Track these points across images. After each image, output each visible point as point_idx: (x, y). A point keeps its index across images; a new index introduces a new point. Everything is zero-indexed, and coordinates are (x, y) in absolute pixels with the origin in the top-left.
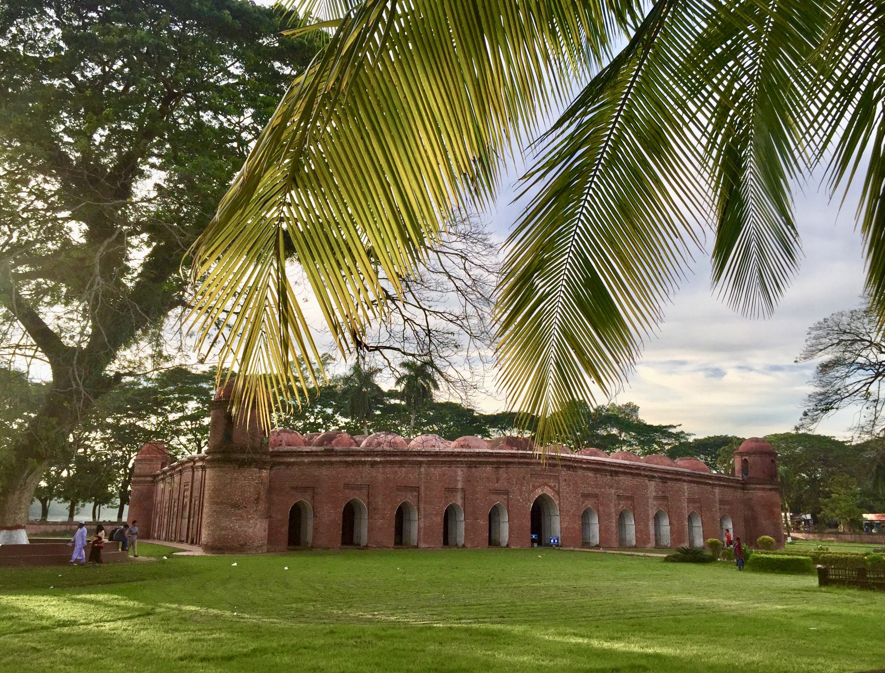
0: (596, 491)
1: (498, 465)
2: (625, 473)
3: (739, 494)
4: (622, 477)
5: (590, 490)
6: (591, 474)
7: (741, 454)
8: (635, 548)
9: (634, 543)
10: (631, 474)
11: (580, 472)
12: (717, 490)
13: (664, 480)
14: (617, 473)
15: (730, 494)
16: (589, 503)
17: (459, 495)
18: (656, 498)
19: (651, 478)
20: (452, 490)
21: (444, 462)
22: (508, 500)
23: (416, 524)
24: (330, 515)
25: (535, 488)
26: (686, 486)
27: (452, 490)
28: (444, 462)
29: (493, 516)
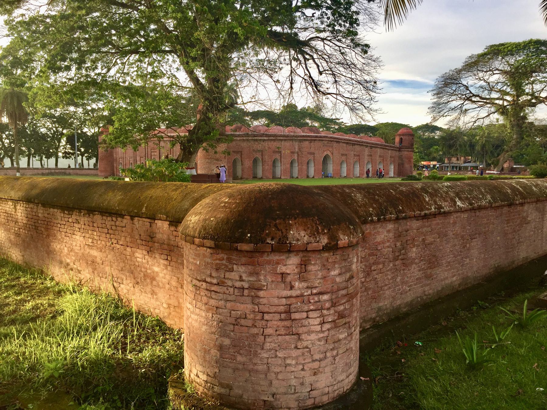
0: (346, 153)
1: (311, 141)
2: (357, 144)
4: (356, 146)
5: (344, 152)
6: (345, 145)
10: (360, 145)
11: (341, 144)
13: (371, 147)
14: (355, 144)
16: (344, 158)
17: (296, 155)
25: (324, 151)
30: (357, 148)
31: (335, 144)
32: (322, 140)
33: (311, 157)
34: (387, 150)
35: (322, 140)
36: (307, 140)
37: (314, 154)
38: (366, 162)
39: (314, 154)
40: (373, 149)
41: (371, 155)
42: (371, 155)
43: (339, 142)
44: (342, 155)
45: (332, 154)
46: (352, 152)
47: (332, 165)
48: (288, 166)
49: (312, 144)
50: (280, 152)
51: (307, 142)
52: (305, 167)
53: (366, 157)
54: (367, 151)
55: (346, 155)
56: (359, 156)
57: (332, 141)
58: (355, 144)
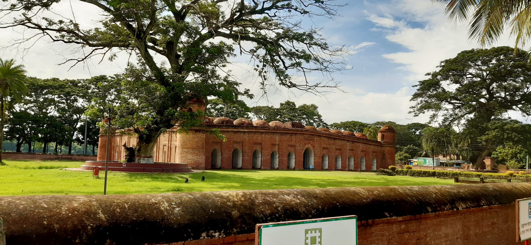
0: (328, 146)
3: (380, 149)
6: (326, 139)
9: (340, 168)
11: (323, 138)
12: (372, 147)
15: (376, 148)
16: (325, 152)
17: (277, 147)
18: (350, 150)
19: (349, 141)
20: (274, 145)
21: (272, 132)
22: (295, 149)
23: (260, 159)
24: (228, 154)
25: (305, 144)
26: (361, 145)
27: (274, 145)
28: (272, 132)
29: (289, 155)
30: (339, 142)
31: (316, 138)
32: (303, 134)
33: (291, 150)
34: (368, 146)
35: (303, 134)
36: (288, 133)
37: (294, 146)
38: (348, 156)
39: (294, 146)
40: (355, 144)
41: (353, 150)
42: (353, 150)
43: (320, 136)
44: (324, 148)
45: (314, 147)
46: (334, 146)
47: (313, 158)
48: (269, 157)
49: (293, 137)
50: (261, 144)
51: (288, 136)
52: (285, 159)
53: (348, 151)
54: (348, 145)
55: (327, 148)
56: (340, 150)
57: (313, 135)
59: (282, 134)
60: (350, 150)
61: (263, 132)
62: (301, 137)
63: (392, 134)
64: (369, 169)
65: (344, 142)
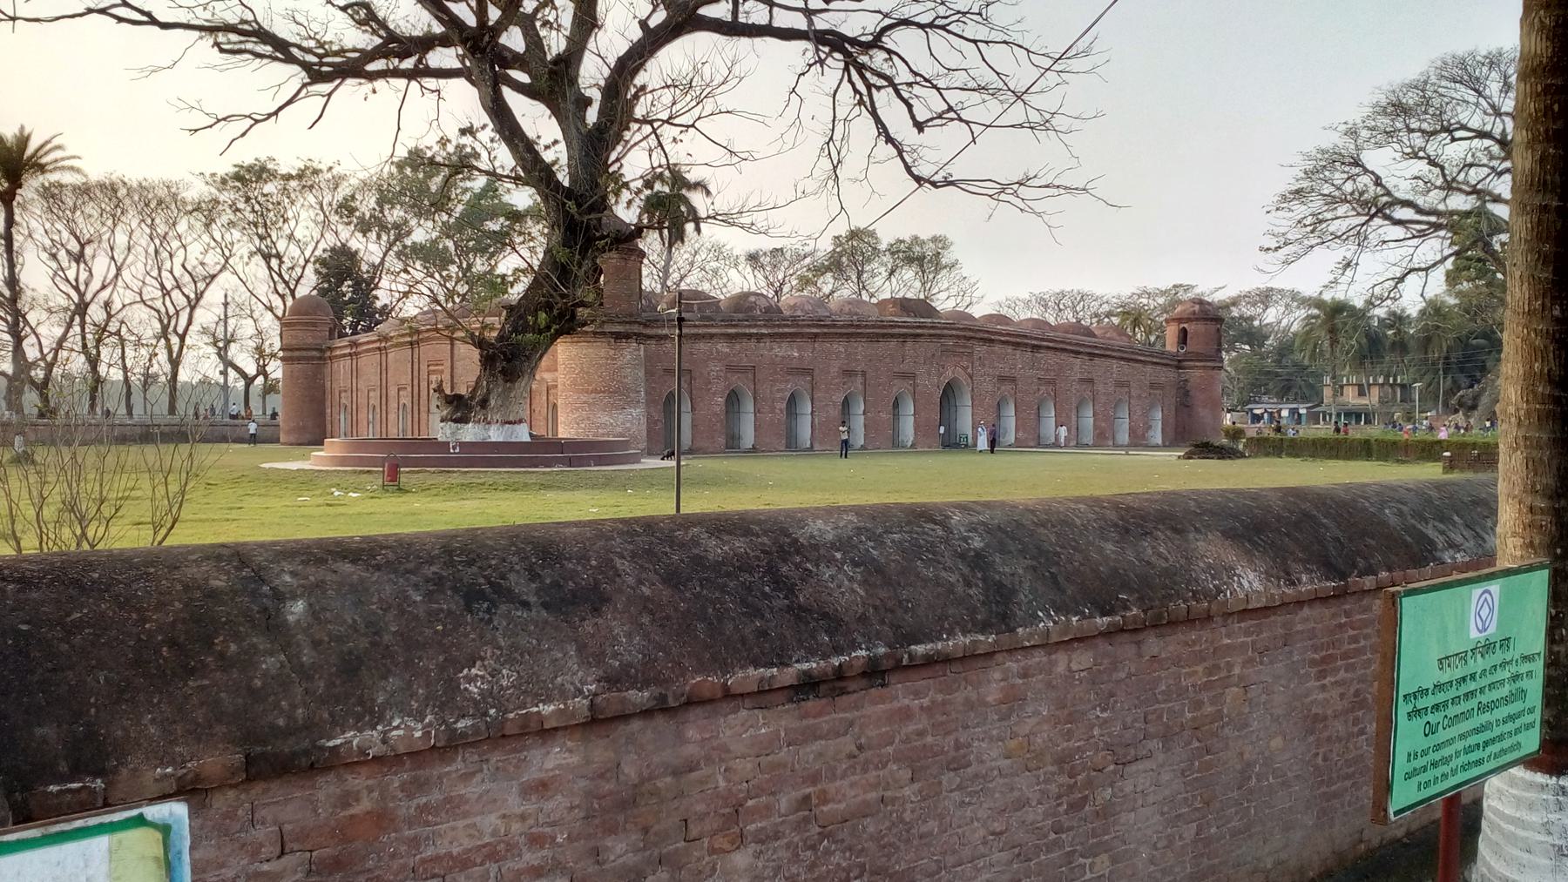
6: (1009, 349)
7: (1179, 320)
8: (1095, 446)
11: (997, 348)
16: (1007, 388)
21: (841, 335)
28: (841, 335)
30: (1051, 359)
31: (980, 349)
32: (940, 336)
35: (940, 336)
36: (892, 336)
40: (1097, 361)
42: (1091, 381)
44: (1002, 379)
49: (909, 344)
51: (893, 343)
55: (1013, 380)
56: (1051, 382)
58: (1039, 347)
59: (876, 338)
60: (1082, 381)
61: (816, 335)
62: (932, 347)
63: (1212, 327)
64: (1139, 441)
65: (1064, 356)
